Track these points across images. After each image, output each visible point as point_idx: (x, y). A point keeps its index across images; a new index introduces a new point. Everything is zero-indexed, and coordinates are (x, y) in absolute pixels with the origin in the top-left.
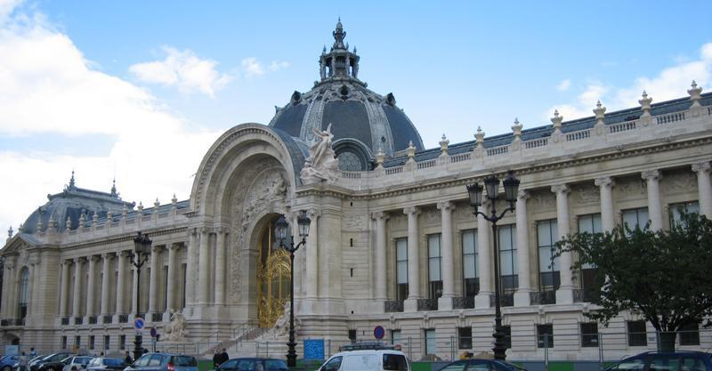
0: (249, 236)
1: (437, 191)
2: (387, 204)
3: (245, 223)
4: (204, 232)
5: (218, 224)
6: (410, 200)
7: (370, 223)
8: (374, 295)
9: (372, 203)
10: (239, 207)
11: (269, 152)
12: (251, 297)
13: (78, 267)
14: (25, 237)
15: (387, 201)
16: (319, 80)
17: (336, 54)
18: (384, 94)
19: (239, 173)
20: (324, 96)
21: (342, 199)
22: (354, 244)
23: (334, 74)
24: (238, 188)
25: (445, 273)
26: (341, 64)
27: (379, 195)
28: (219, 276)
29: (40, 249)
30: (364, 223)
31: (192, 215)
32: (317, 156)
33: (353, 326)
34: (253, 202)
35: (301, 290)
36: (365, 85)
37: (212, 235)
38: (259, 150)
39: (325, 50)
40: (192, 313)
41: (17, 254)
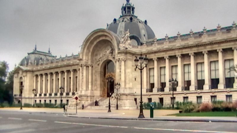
3: (98, 63)
4: (85, 66)
5: (89, 63)
10: (96, 57)
11: (107, 38)
12: (101, 87)
13: (39, 77)
14: (21, 67)
16: (122, 15)
17: (127, 6)
18: (144, 20)
19: (96, 46)
20: (124, 20)
23: (127, 13)
25: (206, 77)
26: (129, 10)
28: (90, 80)
29: (26, 71)
31: (81, 60)
32: (124, 40)
33: (136, 97)
34: (101, 56)
36: (137, 17)
37: (87, 67)
38: (104, 38)
39: (123, 5)
40: (81, 92)
41: (18, 73)
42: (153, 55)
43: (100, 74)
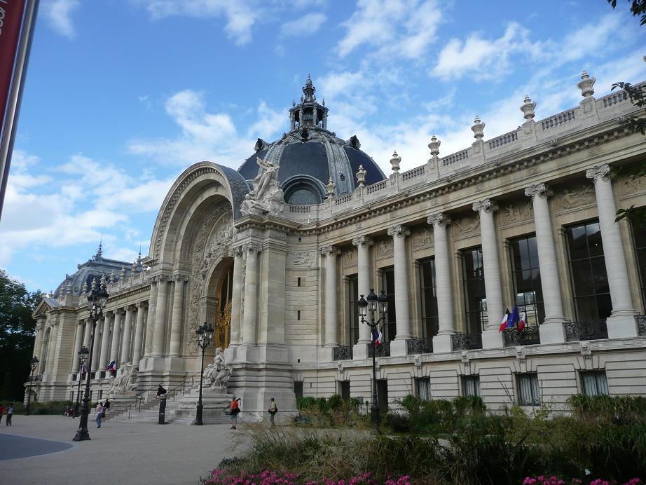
0: (207, 284)
1: (389, 215)
2: (335, 237)
6: (359, 229)
7: (320, 259)
8: (324, 340)
9: (322, 237)
10: (199, 255)
15: (337, 233)
19: (197, 220)
21: (287, 234)
22: (301, 283)
24: (198, 236)
26: (309, 116)
27: (328, 227)
30: (313, 260)
33: (299, 378)
35: (239, 335)
41: (45, 317)
42: (353, 228)
43: (208, 303)
